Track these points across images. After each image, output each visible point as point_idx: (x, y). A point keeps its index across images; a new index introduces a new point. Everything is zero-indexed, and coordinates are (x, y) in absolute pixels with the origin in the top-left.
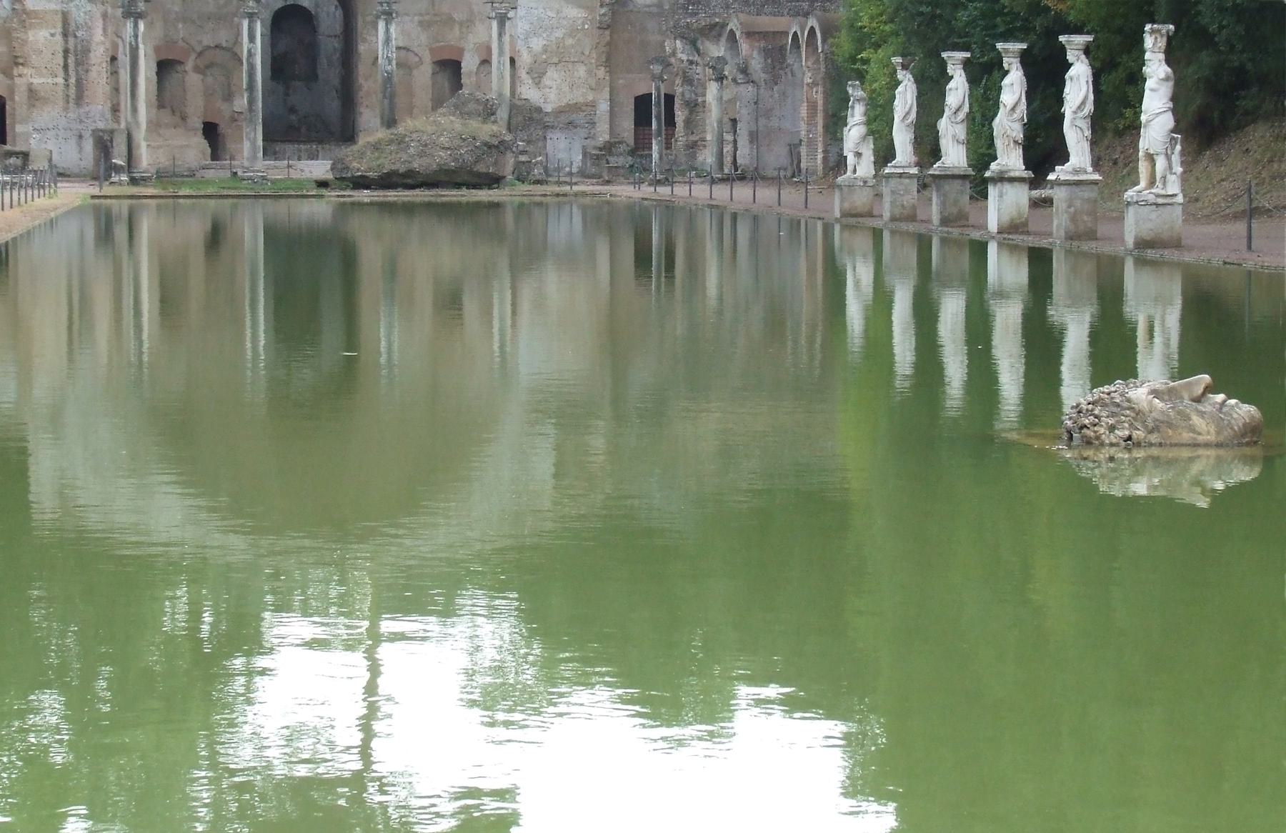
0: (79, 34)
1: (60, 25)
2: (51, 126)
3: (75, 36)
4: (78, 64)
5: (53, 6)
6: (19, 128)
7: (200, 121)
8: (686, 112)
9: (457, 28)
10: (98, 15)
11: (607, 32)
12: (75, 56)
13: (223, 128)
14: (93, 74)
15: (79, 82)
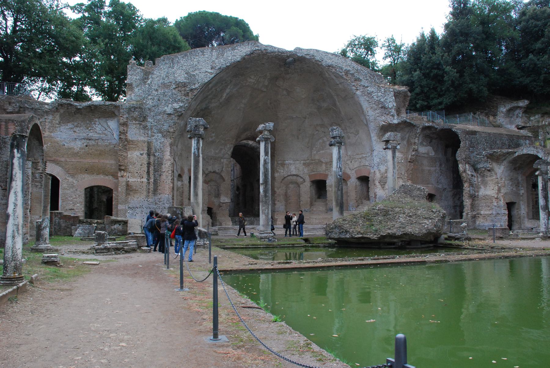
0: (157, 154)
1: (146, 149)
2: (138, 206)
3: (154, 156)
4: (155, 171)
5: (142, 138)
6: (120, 207)
7: (206, 206)
8: (471, 200)
9: (324, 165)
10: (168, 144)
11: (412, 164)
12: (154, 167)
13: (215, 210)
14: (164, 177)
15: (155, 182)
